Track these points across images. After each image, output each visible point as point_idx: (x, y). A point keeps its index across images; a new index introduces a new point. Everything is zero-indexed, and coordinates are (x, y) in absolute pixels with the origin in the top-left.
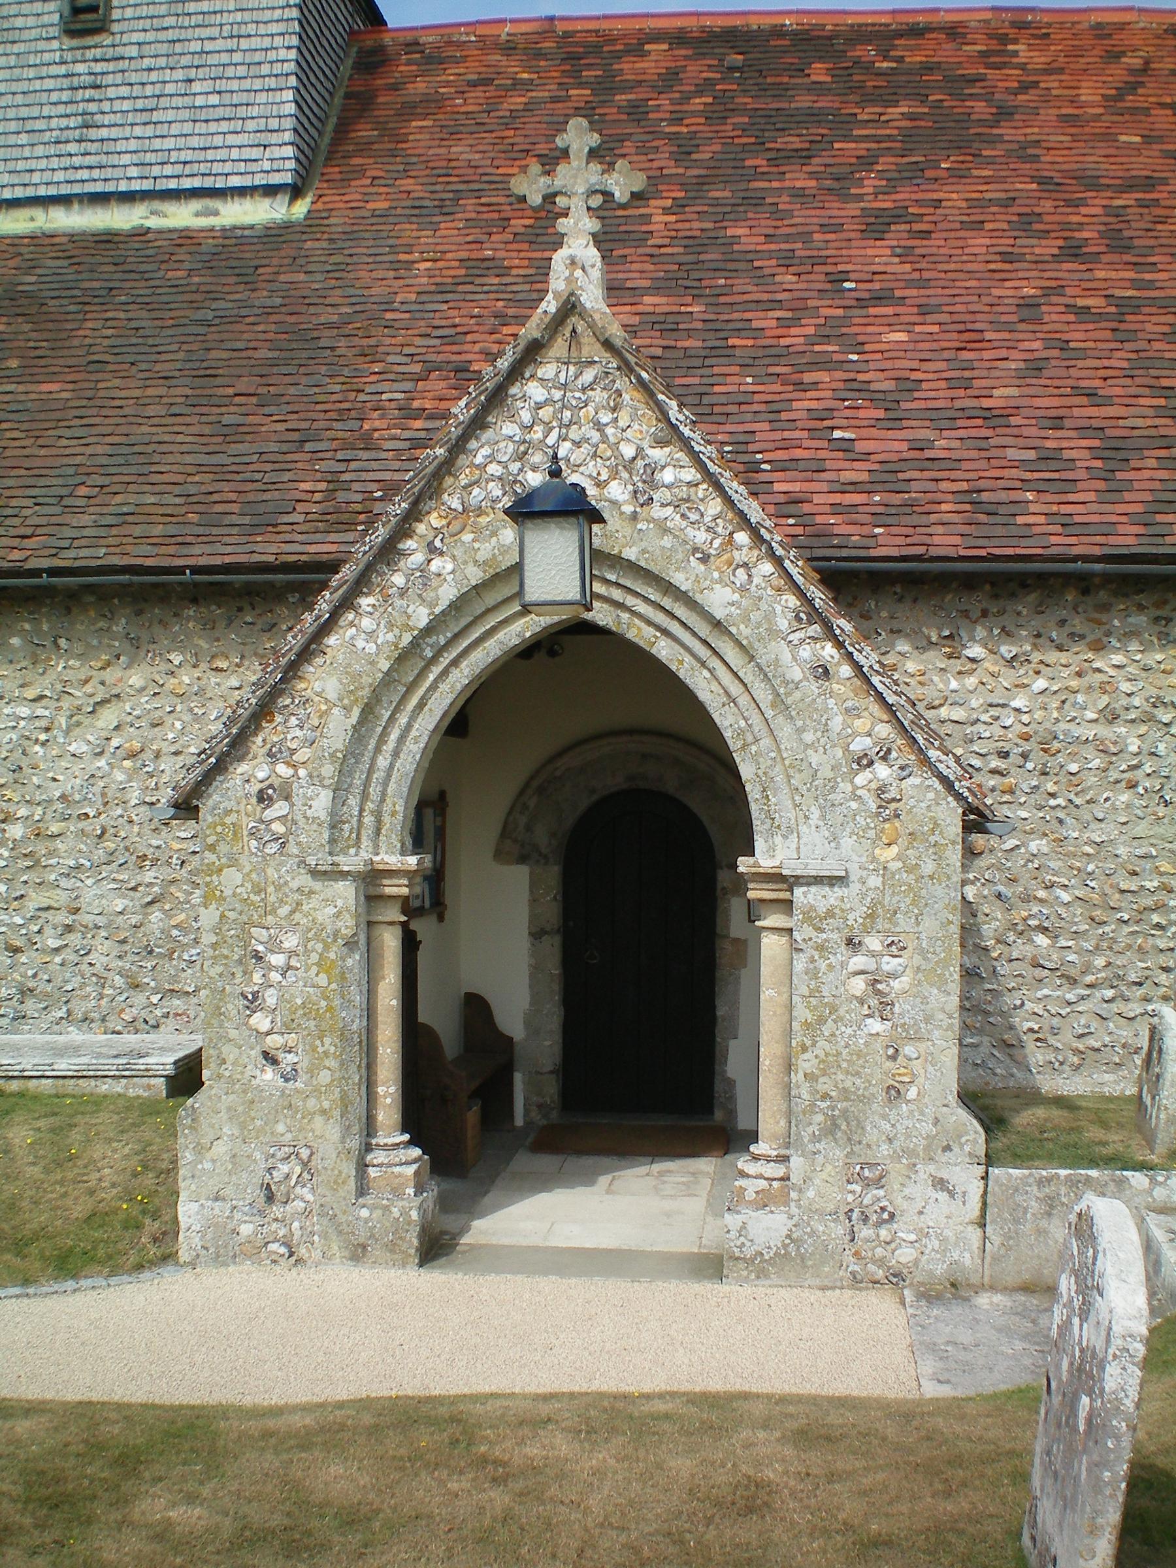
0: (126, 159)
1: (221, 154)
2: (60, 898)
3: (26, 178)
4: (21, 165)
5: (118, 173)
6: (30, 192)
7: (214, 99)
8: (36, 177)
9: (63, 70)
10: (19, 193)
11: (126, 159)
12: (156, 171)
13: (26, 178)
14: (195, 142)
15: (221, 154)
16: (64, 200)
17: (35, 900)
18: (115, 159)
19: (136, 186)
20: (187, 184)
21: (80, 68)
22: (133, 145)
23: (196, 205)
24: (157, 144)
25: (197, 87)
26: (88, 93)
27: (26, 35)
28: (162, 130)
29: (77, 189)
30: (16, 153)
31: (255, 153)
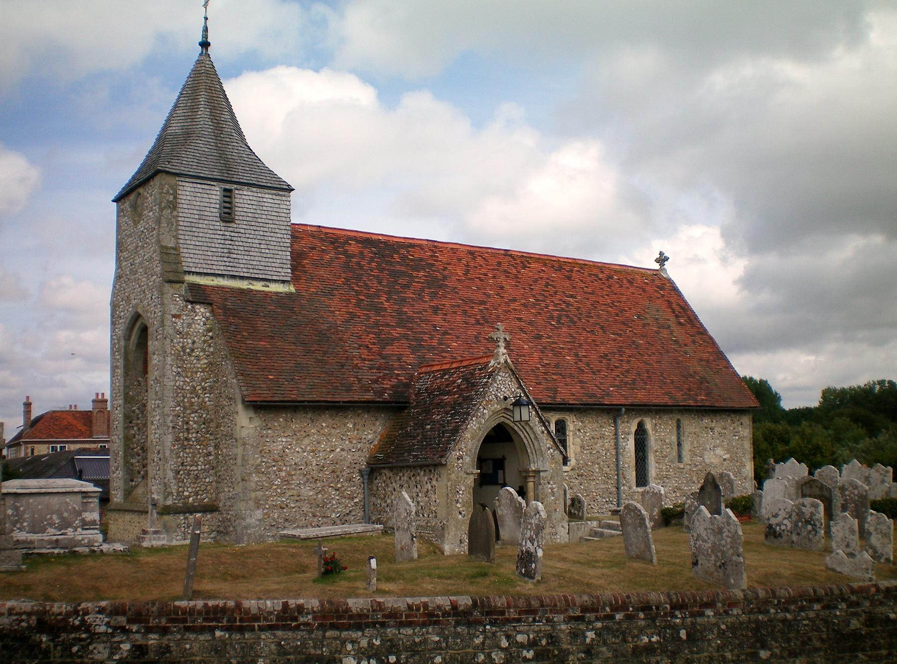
0: (242, 266)
1: (270, 269)
2: (295, 492)
3: (211, 267)
4: (209, 262)
5: (240, 270)
6: (212, 272)
7: (267, 251)
8: (214, 267)
9: (221, 233)
10: (209, 271)
11: (242, 266)
12: (251, 271)
13: (211, 267)
14: (263, 264)
15: (270, 269)
16: (222, 276)
17: (289, 493)
18: (238, 265)
19: (246, 275)
20: (261, 276)
21: (226, 233)
22: (244, 262)
23: (262, 283)
24: (251, 262)
25: (262, 246)
26: (230, 242)
27: (208, 218)
28: (252, 258)
29: (227, 273)
30: (208, 258)
31: (280, 270)
